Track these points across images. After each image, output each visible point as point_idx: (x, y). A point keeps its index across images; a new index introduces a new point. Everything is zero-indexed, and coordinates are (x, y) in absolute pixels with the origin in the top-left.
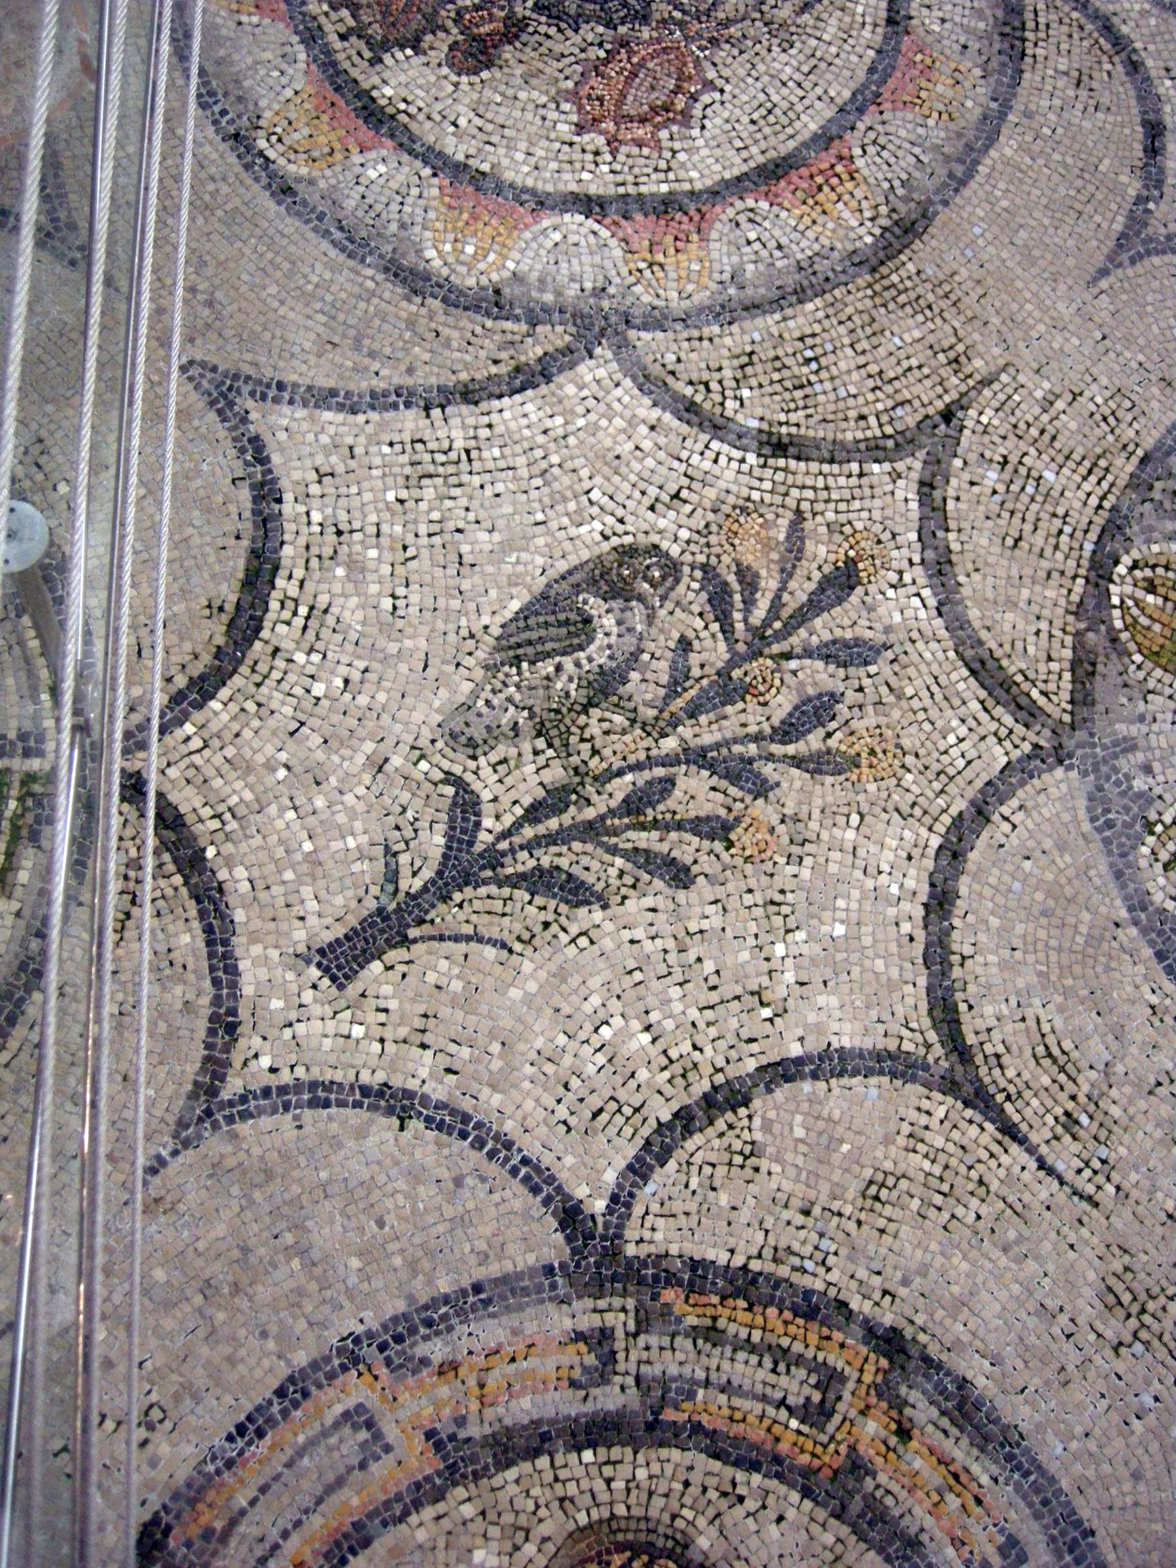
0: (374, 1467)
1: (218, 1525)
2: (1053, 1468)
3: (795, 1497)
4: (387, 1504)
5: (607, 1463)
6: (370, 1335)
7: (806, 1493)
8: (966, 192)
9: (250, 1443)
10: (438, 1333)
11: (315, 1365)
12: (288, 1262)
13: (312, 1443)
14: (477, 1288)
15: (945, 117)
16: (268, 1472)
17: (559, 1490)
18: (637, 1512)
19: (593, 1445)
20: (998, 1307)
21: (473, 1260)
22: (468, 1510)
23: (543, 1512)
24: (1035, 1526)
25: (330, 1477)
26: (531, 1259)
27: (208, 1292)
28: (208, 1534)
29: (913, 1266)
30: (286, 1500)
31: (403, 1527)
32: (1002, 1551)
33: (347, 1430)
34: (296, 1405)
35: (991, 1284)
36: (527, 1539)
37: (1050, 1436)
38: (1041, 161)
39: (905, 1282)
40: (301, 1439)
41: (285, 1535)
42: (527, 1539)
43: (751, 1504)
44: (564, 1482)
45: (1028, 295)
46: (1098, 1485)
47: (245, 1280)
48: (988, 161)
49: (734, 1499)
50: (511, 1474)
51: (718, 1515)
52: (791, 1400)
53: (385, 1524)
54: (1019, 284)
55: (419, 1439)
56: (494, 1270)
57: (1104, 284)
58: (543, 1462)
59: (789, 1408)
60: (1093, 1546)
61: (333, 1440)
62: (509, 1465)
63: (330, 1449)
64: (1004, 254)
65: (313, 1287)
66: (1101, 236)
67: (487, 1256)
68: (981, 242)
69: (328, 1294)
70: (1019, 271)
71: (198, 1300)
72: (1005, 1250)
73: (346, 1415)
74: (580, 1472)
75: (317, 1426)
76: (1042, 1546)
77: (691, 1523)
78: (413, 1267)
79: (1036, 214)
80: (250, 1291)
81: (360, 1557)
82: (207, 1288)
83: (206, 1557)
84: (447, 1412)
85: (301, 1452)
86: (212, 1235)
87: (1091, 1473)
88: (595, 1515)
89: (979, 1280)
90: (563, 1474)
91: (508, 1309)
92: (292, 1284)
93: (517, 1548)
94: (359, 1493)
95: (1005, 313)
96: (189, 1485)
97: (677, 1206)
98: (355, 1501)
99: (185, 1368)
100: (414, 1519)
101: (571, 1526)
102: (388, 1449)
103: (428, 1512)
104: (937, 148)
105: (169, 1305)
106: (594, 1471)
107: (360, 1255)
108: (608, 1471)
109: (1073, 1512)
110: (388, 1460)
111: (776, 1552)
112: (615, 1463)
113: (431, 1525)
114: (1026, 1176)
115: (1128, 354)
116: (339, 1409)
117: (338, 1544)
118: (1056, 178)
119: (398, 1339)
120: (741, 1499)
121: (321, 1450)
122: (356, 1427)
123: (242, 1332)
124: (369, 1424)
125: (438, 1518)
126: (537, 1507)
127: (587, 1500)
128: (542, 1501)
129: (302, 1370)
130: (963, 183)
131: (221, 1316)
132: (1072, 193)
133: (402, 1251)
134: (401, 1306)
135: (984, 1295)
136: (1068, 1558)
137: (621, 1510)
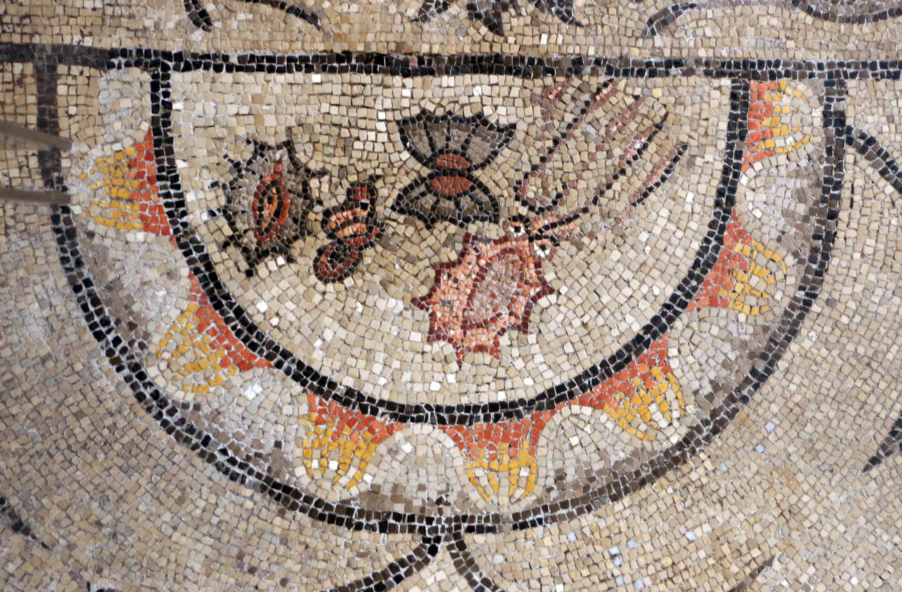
8: (765, 388)
15: (756, 311)
38: (835, 353)
45: (806, 487)
48: (787, 356)
54: (800, 477)
57: (874, 472)
64: (791, 449)
66: (879, 425)
68: (772, 437)
70: (801, 464)
79: (824, 407)
95: (785, 506)
104: (744, 344)
115: (885, 537)
118: (847, 369)
130: (763, 378)
132: (859, 383)
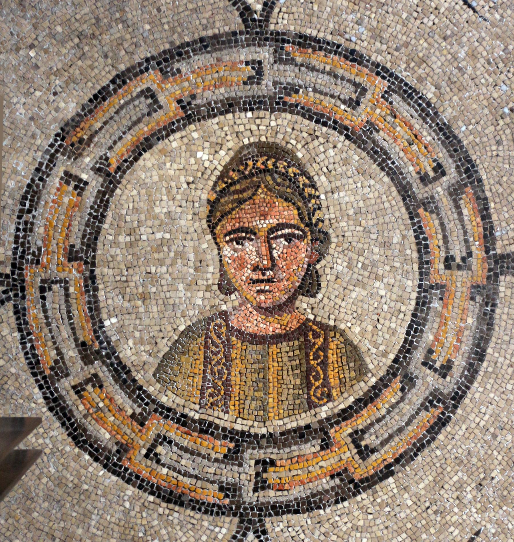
0: (154, 115)
1: (86, 137)
2: (461, 136)
3: (342, 138)
4: (160, 131)
5: (258, 118)
6: (153, 58)
7: (347, 137)
9: (99, 103)
10: (184, 59)
11: (128, 70)
12: (117, 25)
13: (127, 103)
14: (202, 40)
16: (107, 115)
17: (236, 128)
18: (271, 140)
19: (252, 110)
20: (439, 64)
21: (200, 27)
22: (195, 135)
23: (229, 138)
24: (450, 160)
25: (134, 118)
26: (227, 29)
27: (81, 37)
28: (81, 141)
29: (401, 43)
30: (115, 127)
31: (166, 141)
32: (435, 170)
33: (142, 99)
34: (120, 87)
35: (437, 53)
36: (221, 149)
37: (460, 123)
39: (397, 49)
40: (122, 102)
41: (115, 143)
42: (221, 149)
43: (321, 140)
44: (239, 125)
46: (481, 145)
47: (97, 33)
49: (314, 136)
50: (216, 120)
51: (307, 143)
52: (342, 97)
53: (158, 139)
55: (174, 105)
56: (210, 33)
58: (230, 116)
59: (340, 99)
60: (477, 172)
61: (136, 103)
62: (215, 116)
63: (135, 107)
65: (128, 36)
67: (207, 27)
69: (135, 40)
71: (76, 40)
72: (445, 39)
73: (142, 92)
74: (245, 121)
75: (129, 97)
76: (453, 170)
77: (295, 147)
78: (173, 30)
80: (100, 38)
81: (147, 153)
82: (80, 36)
83: (80, 151)
84: (187, 93)
85: (122, 107)
86: (83, 12)
87: (477, 140)
88: (252, 140)
89: (432, 51)
90: (238, 122)
91: (216, 50)
92: (119, 35)
93: (216, 152)
94: (147, 126)
96: (73, 120)
97: (294, 9)
98: (146, 129)
99: (71, 70)
100: (171, 138)
101: (241, 144)
102: (160, 107)
103: (178, 135)
105: (63, 43)
106: (252, 121)
107: (149, 23)
108: (258, 121)
109: (468, 156)
110: (161, 112)
111: (332, 161)
112: (261, 118)
113: (178, 140)
114: (457, 7)
116: (139, 90)
117: (138, 147)
119: (166, 60)
120: (317, 137)
121: (131, 106)
122: (146, 97)
123: (96, 55)
124: (153, 96)
125: (182, 138)
126: (226, 135)
127: (249, 133)
128: (228, 133)
129: (123, 73)
131: (86, 48)
133: (168, 22)
134: (167, 46)
135: (434, 59)
136: (464, 176)
137: (263, 139)
